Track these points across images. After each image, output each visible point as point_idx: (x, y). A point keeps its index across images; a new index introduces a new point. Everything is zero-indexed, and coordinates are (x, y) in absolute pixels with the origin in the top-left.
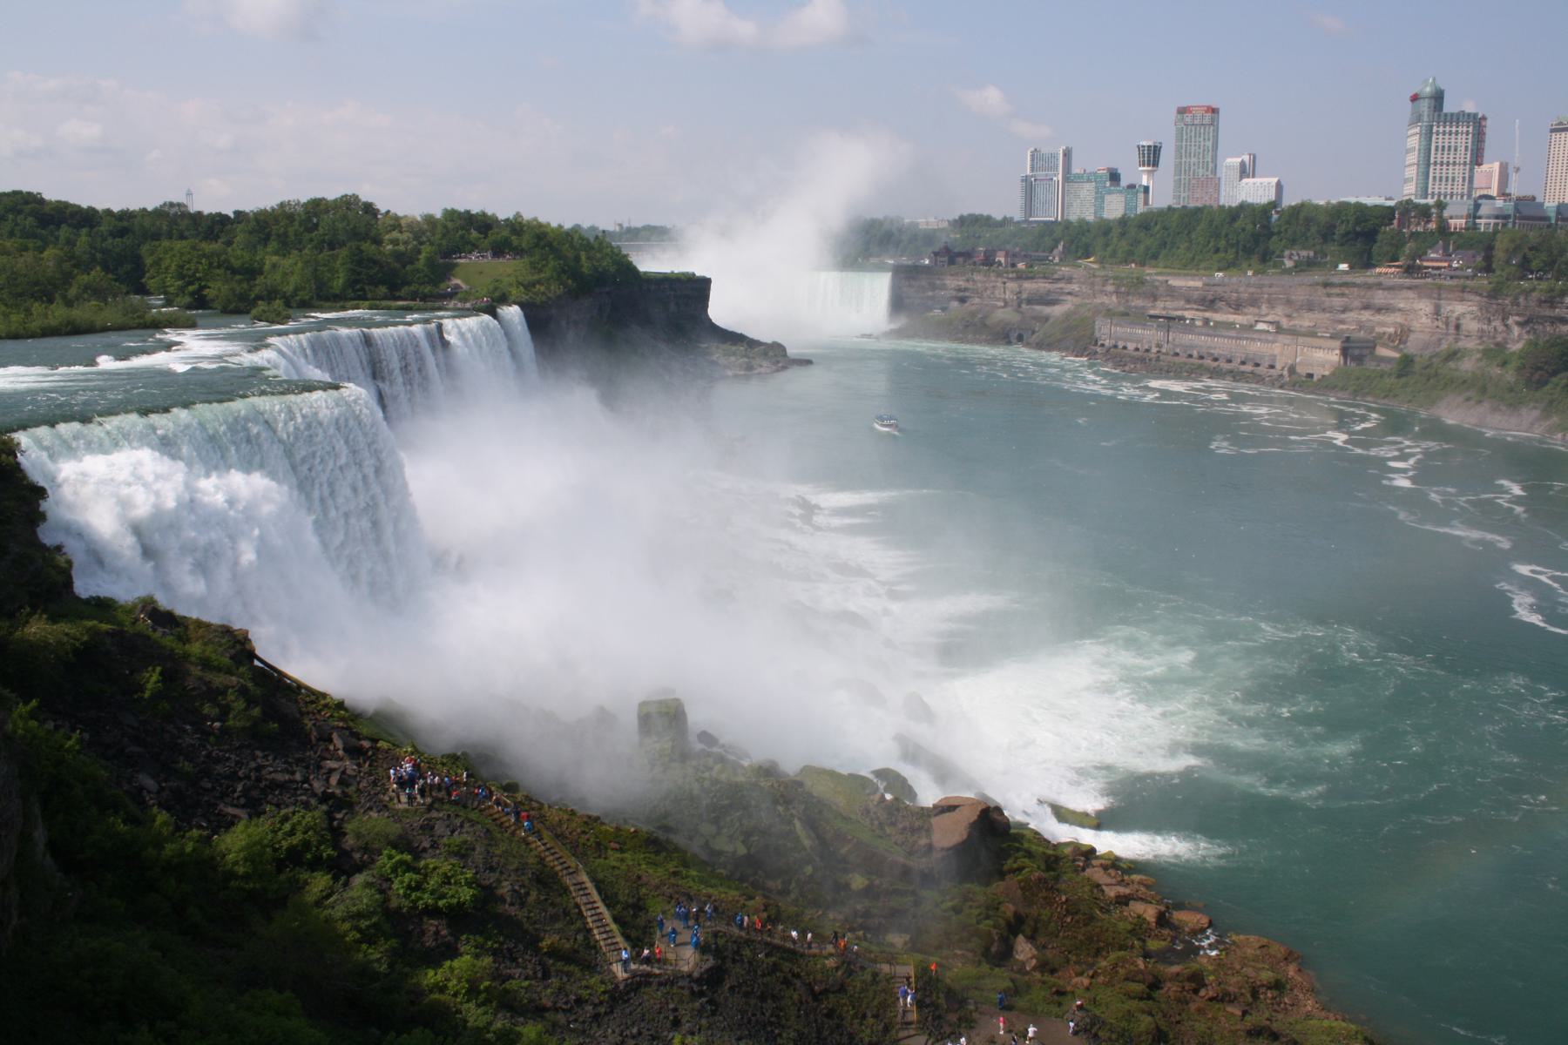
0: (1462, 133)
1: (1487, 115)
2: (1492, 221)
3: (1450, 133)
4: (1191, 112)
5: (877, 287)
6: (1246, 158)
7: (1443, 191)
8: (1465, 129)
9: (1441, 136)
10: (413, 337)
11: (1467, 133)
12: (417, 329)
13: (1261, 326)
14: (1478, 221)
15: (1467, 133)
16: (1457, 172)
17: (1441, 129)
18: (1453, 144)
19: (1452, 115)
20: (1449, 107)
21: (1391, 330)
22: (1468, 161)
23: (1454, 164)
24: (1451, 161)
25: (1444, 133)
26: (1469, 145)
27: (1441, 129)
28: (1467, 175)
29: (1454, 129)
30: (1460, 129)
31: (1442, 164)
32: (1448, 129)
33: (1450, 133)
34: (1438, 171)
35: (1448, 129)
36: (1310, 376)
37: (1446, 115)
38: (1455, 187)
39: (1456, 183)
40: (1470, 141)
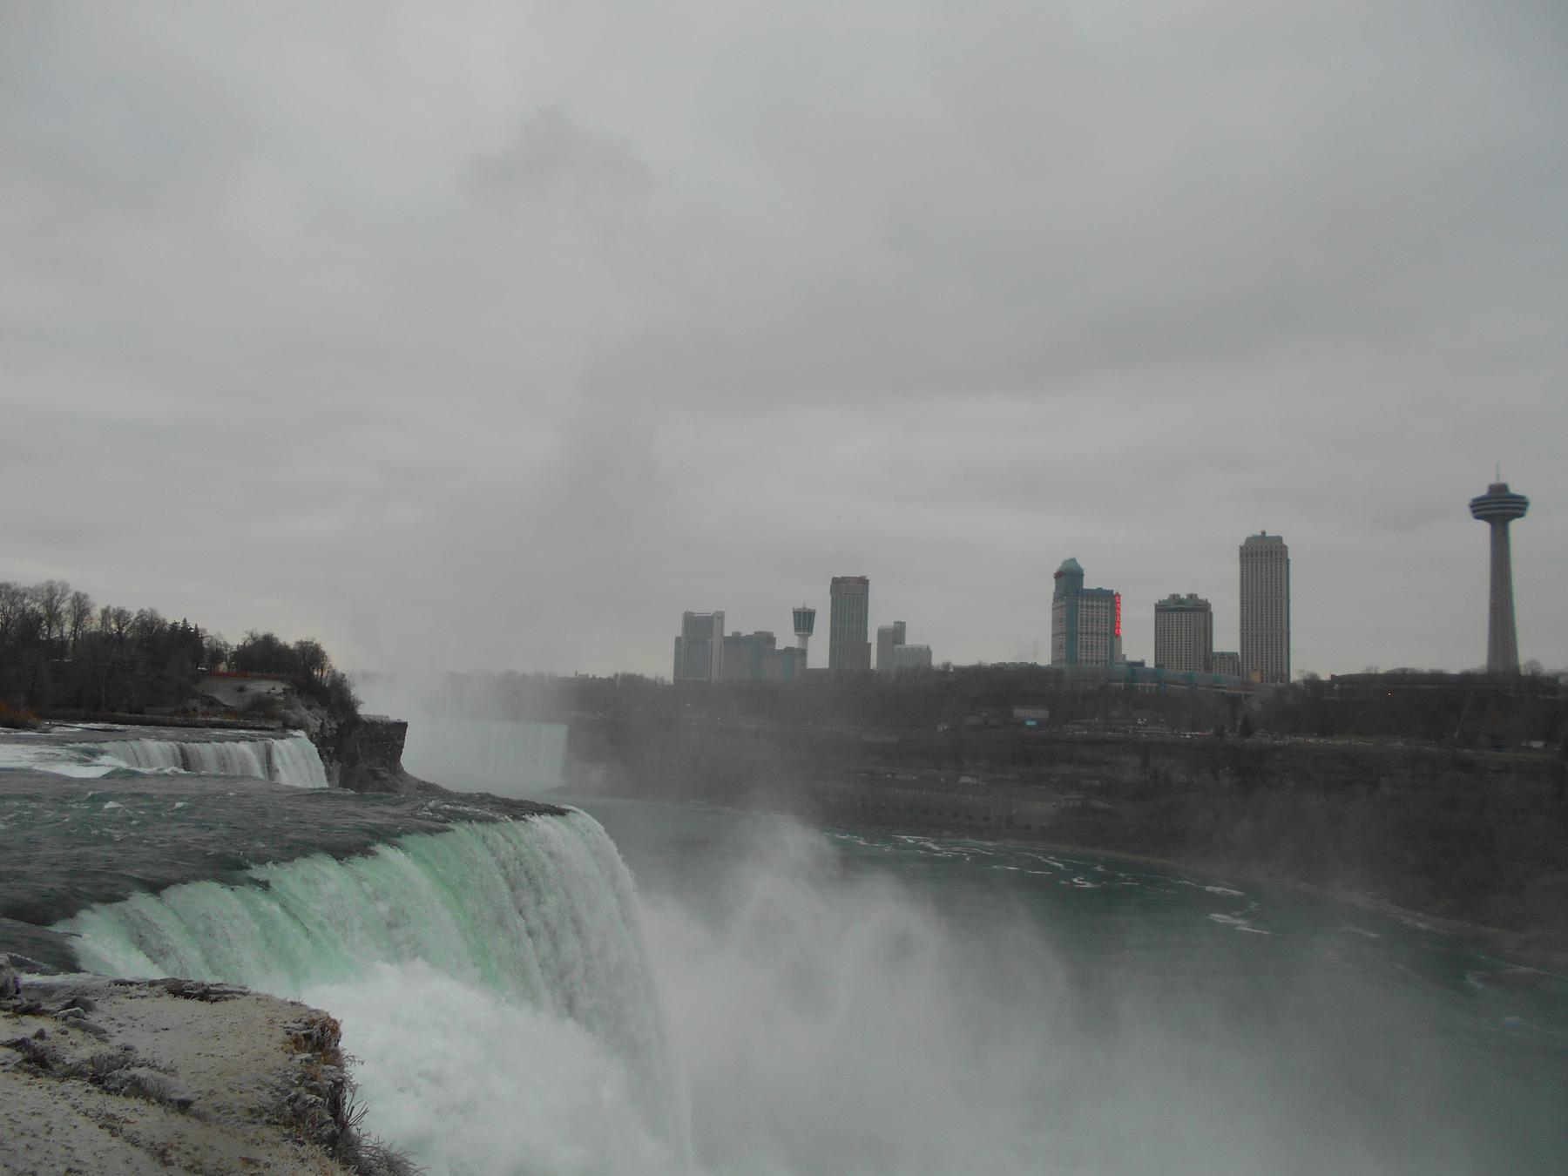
0: (1102, 607)
1: (1120, 593)
2: (1155, 685)
5: (557, 734)
6: (898, 626)
7: (1089, 658)
10: (244, 758)
12: (244, 747)
13: (964, 779)
14: (1134, 684)
15: (1106, 608)
17: (1085, 603)
18: (1095, 617)
19: (1092, 591)
20: (1089, 583)
21: (1098, 782)
22: (1108, 632)
23: (1097, 634)
24: (1095, 631)
26: (1108, 617)
27: (1085, 603)
28: (1108, 644)
30: (1100, 604)
32: (1090, 603)
35: (1090, 603)
36: (1029, 827)
40: (1108, 615)
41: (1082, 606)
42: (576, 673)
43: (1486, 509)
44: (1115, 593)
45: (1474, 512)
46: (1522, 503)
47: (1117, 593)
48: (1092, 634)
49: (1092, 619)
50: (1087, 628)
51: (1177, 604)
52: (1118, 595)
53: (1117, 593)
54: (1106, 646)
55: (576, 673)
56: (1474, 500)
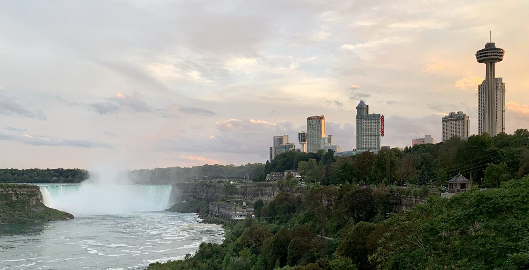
0: (373, 123)
3: (368, 123)
4: (312, 119)
8: (374, 121)
9: (365, 124)
11: (375, 123)
15: (375, 123)
16: (372, 139)
17: (365, 122)
23: (371, 136)
25: (366, 123)
27: (365, 122)
29: (370, 121)
31: (366, 136)
32: (367, 121)
33: (368, 123)
34: (365, 139)
35: (367, 121)
37: (369, 115)
38: (372, 145)
39: (372, 144)
40: (377, 126)
41: (363, 123)
42: (242, 164)
43: (481, 57)
44: (381, 115)
45: (478, 58)
46: (499, 53)
47: (383, 116)
48: (368, 136)
49: (368, 128)
50: (368, 133)
51: (450, 117)
52: (383, 117)
53: (383, 116)
54: (375, 141)
55: (242, 164)
56: (478, 52)
